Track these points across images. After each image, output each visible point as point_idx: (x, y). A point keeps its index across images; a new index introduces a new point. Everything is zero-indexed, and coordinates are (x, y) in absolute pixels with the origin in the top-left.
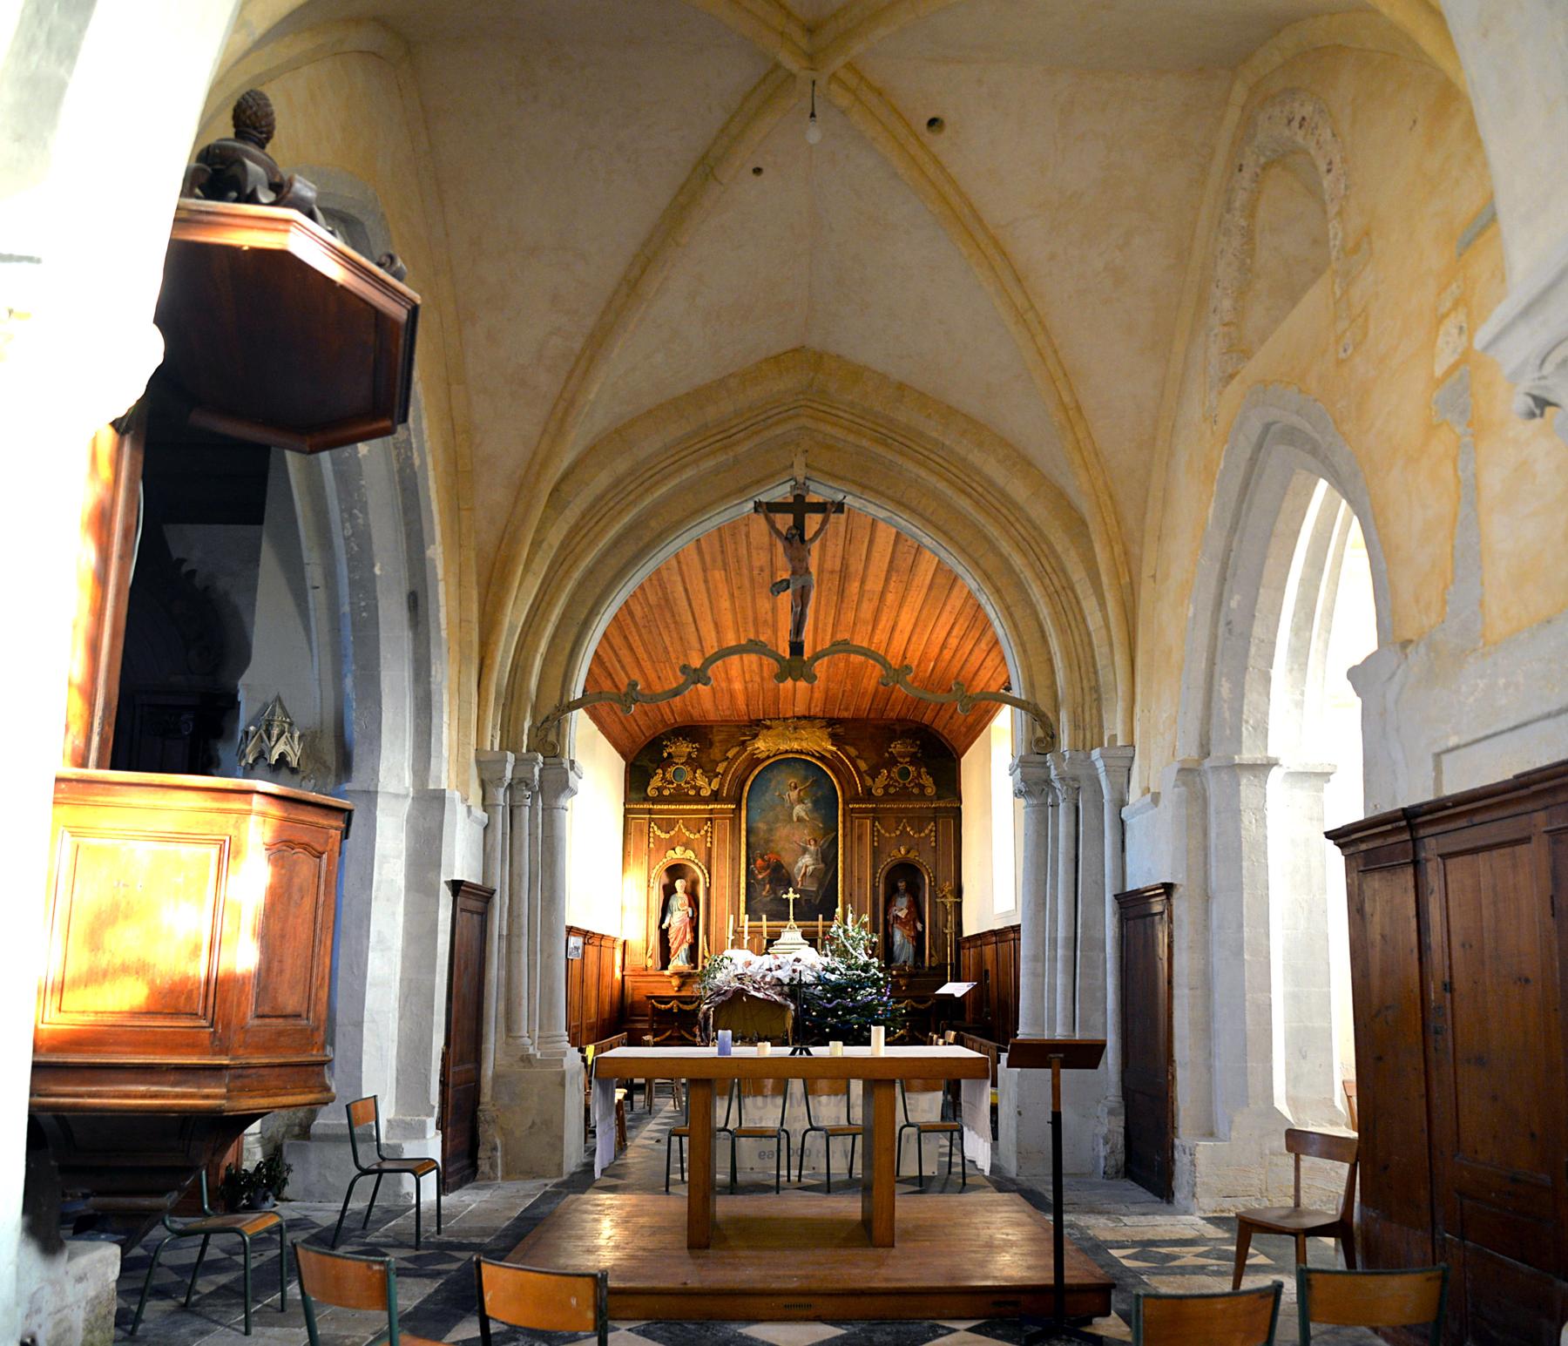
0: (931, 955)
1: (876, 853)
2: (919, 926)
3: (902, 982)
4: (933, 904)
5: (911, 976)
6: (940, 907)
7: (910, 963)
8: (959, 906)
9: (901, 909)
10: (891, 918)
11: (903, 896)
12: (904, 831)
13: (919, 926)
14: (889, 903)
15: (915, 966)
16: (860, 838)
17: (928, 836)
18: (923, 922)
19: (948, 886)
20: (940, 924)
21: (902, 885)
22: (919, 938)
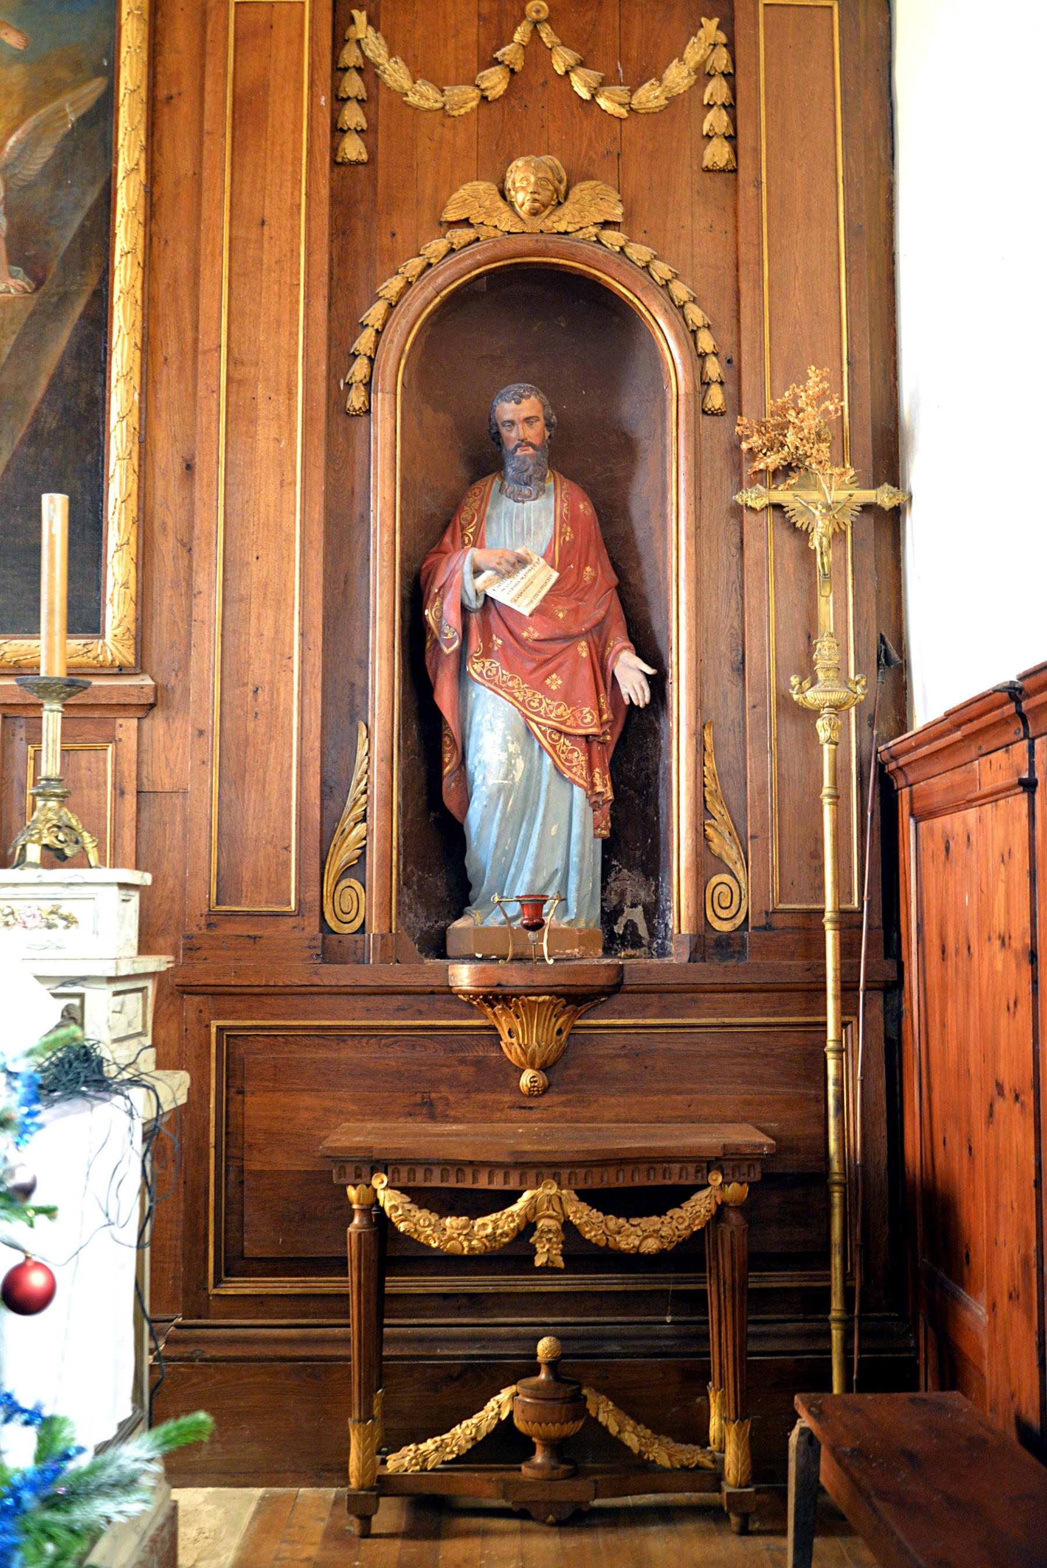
0: (706, 863)
1: (356, 212)
2: (631, 675)
3: (519, 1038)
4: (726, 526)
5: (577, 998)
6: (765, 541)
7: (575, 909)
8: (885, 528)
9: (517, 554)
10: (443, 617)
11: (530, 484)
12: (530, 79)
13: (631, 675)
14: (434, 532)
15: (613, 933)
16: (249, 109)
17: (682, 108)
18: (649, 648)
19: (815, 401)
20: (768, 645)
21: (520, 414)
22: (631, 750)
